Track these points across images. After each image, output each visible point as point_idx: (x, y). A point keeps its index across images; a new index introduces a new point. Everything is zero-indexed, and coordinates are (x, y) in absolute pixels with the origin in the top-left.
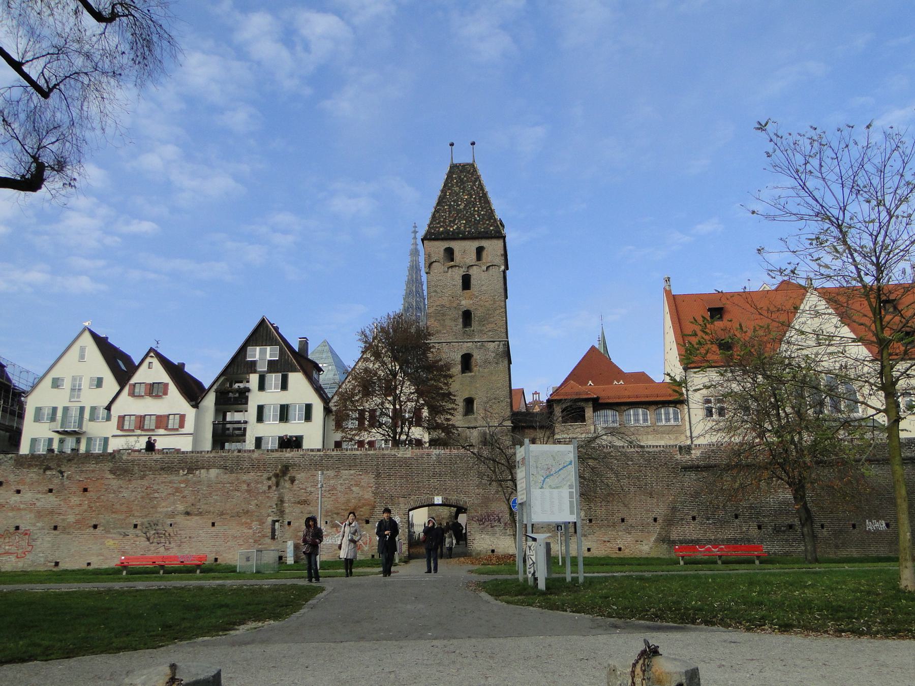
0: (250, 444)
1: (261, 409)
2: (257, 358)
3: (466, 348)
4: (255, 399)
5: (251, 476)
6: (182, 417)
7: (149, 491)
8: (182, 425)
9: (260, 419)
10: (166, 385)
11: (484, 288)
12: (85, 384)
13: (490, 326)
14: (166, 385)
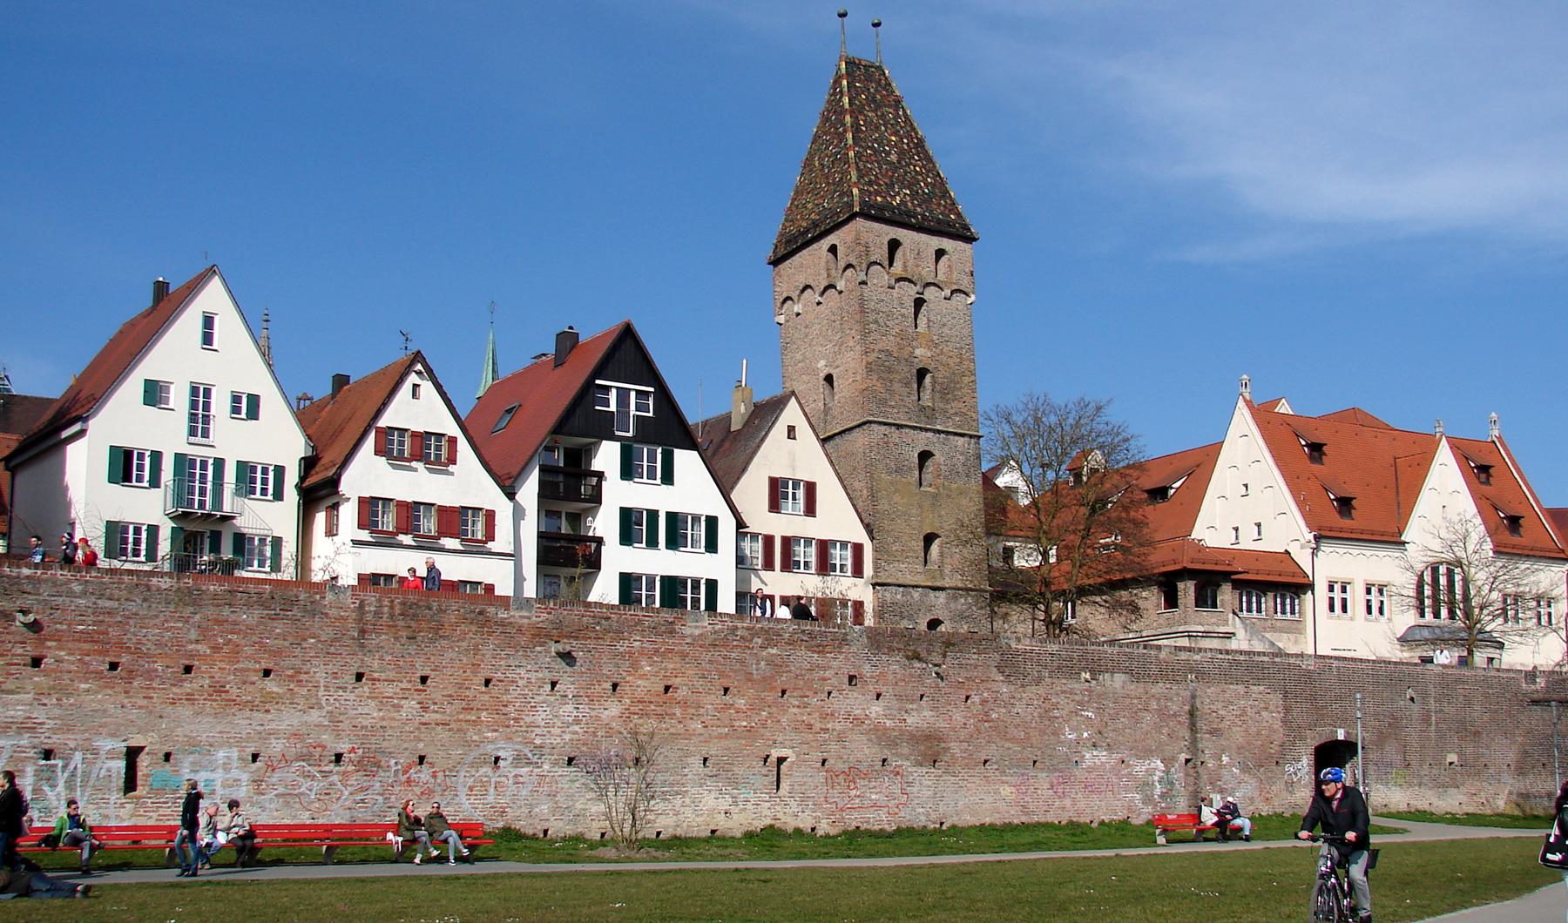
0: (605, 589)
2: (613, 407)
3: (923, 441)
4: (618, 494)
5: (1159, 689)
6: (490, 516)
7: (1047, 705)
8: (490, 536)
9: (627, 538)
10: (453, 441)
11: (946, 330)
12: (220, 405)
14: (453, 441)
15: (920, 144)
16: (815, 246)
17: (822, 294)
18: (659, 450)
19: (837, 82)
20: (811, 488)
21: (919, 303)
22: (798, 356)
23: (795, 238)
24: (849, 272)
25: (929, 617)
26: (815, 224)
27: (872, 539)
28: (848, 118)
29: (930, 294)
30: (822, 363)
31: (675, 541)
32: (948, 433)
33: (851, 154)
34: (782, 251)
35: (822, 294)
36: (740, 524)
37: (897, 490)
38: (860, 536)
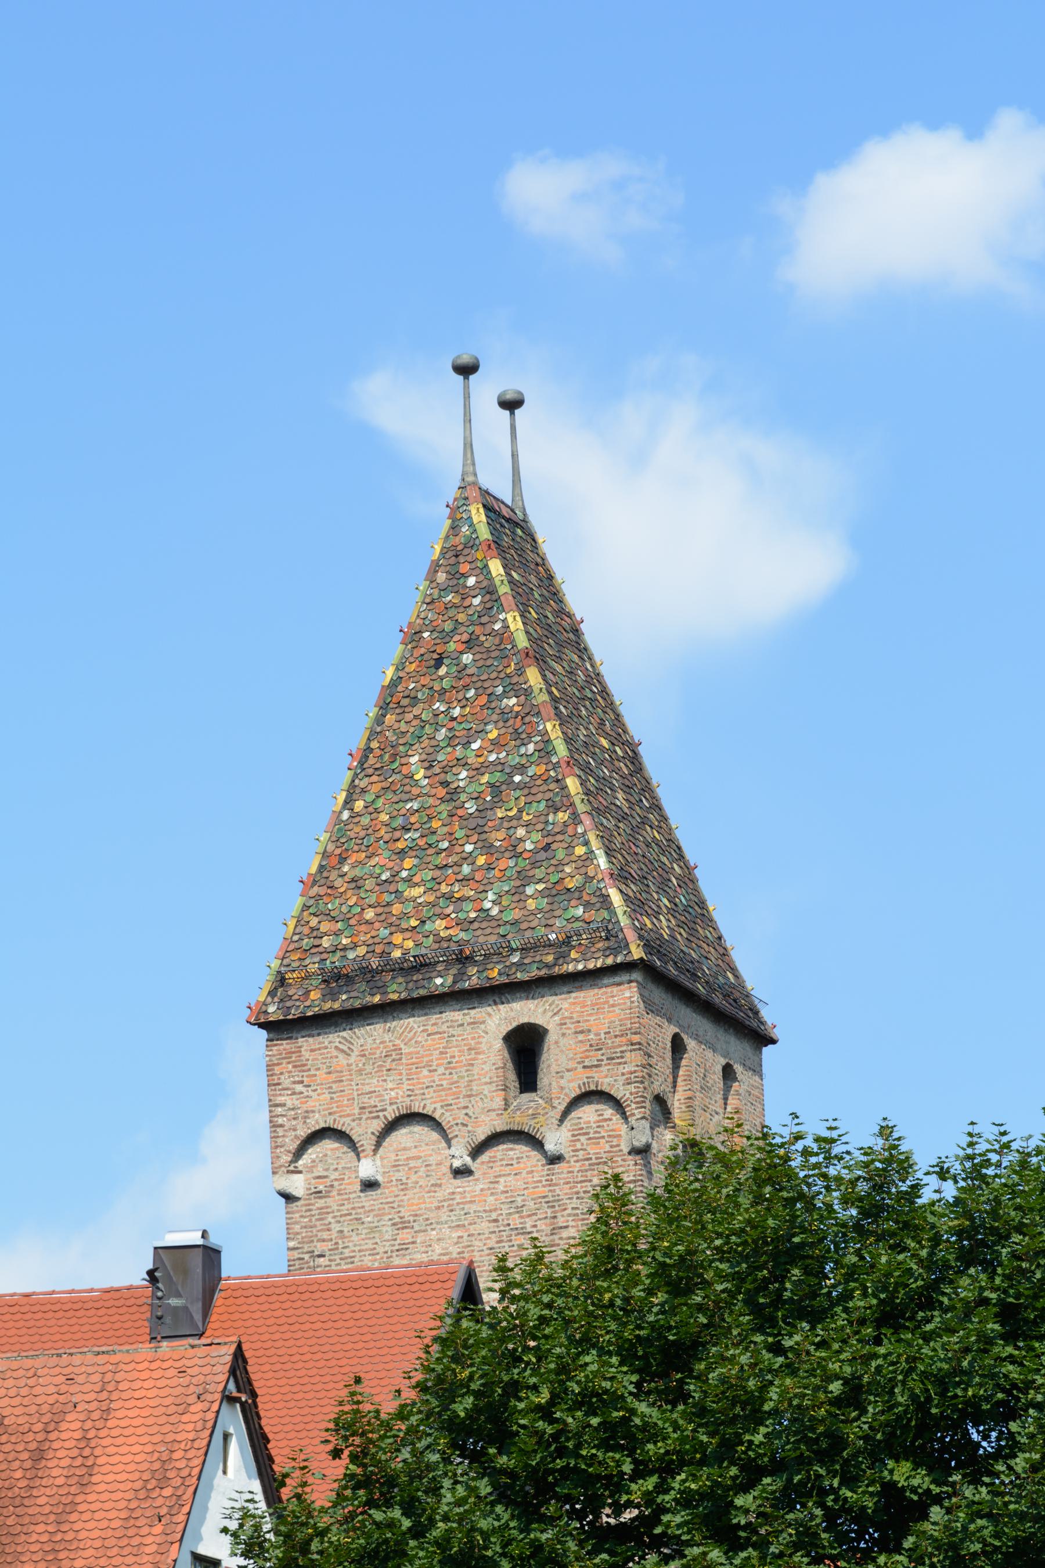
15: (634, 759)
17: (477, 1151)
19: (456, 554)
23: (368, 974)
24: (588, 1113)
26: (463, 960)
28: (533, 676)
33: (572, 784)
34: (316, 1002)
35: (477, 1151)
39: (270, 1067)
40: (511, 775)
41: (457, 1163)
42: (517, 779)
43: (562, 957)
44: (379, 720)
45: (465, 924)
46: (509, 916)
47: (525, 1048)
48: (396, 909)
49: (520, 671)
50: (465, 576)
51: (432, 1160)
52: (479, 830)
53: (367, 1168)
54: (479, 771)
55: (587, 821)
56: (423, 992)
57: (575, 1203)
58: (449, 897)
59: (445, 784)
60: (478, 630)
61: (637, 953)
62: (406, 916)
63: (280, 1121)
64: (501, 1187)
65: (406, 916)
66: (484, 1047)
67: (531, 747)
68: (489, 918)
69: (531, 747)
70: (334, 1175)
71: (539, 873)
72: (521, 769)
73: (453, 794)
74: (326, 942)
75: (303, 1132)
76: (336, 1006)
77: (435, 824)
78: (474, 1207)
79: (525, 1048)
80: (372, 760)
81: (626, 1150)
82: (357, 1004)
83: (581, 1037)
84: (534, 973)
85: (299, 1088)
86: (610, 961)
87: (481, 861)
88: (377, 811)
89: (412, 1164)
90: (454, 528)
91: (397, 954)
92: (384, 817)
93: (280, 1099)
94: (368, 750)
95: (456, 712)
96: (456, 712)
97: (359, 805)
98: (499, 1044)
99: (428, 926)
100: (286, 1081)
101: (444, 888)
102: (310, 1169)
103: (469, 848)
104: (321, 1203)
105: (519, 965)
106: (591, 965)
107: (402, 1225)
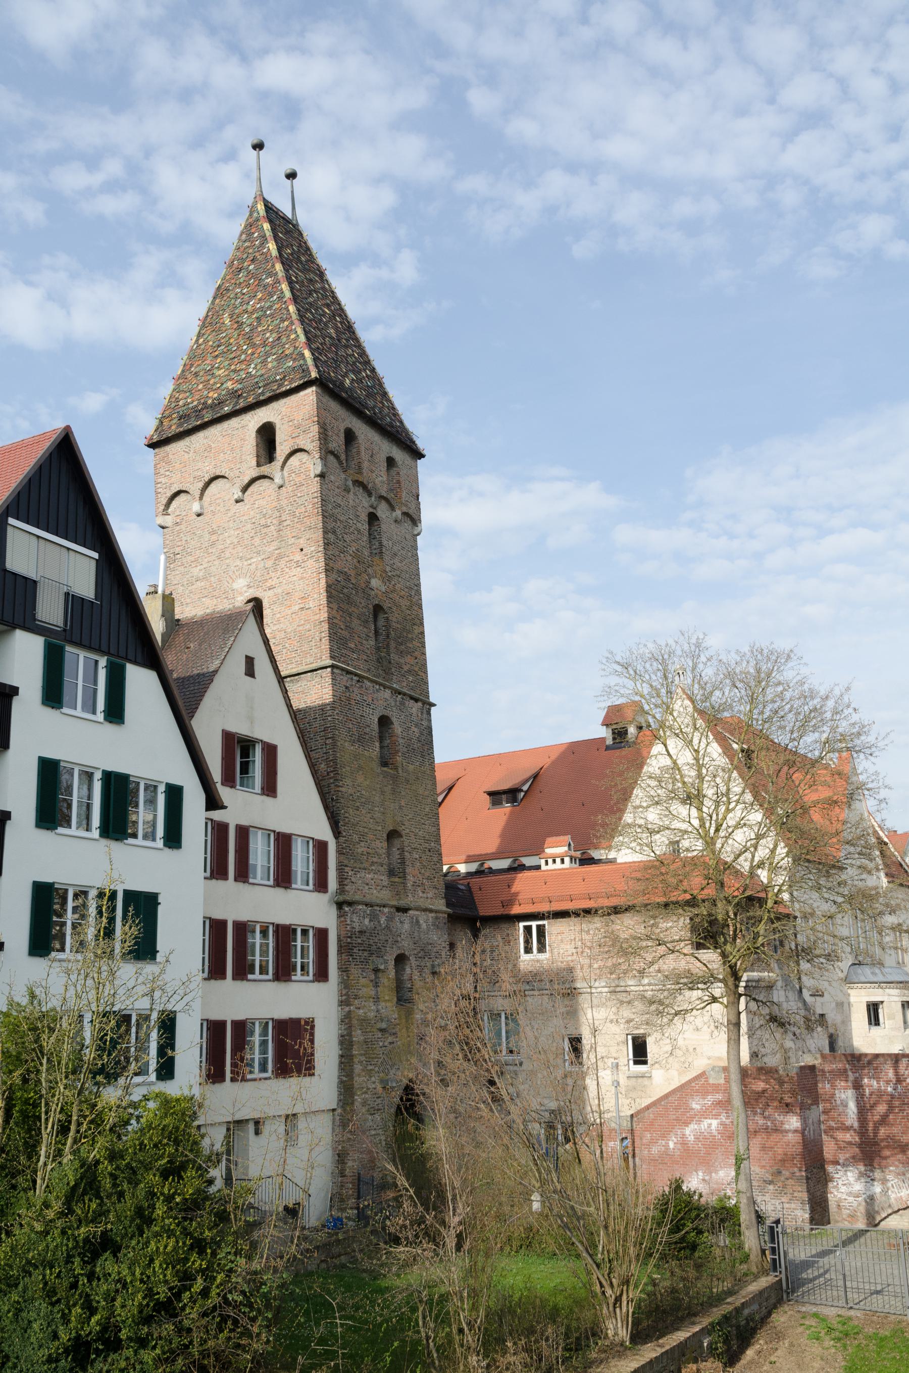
1: (50, 773)
9: (51, 814)
11: (396, 561)
13: (409, 659)
16: (234, 422)
17: (245, 489)
18: (103, 662)
19: (251, 225)
20: (271, 751)
21: (373, 518)
22: (196, 571)
23: (198, 412)
24: (294, 461)
25: (396, 952)
26: (235, 395)
27: (337, 834)
28: (278, 267)
29: (382, 511)
30: (240, 583)
31: (116, 826)
32: (405, 694)
34: (175, 429)
35: (245, 489)
36: (213, 802)
37: (360, 768)
38: (324, 832)
39: (155, 465)
40: (265, 312)
41: (236, 497)
42: (268, 312)
43: (280, 386)
44: (213, 303)
45: (240, 381)
46: (259, 373)
47: (267, 434)
48: (211, 382)
49: (273, 266)
50: (253, 233)
51: (226, 498)
52: (250, 338)
53: (196, 507)
54: (252, 313)
55: (297, 323)
56: (219, 415)
57: (290, 507)
58: (235, 371)
59: (238, 322)
60: (257, 254)
61: (314, 374)
62: (215, 383)
63: (159, 490)
64: (256, 506)
65: (215, 383)
66: (247, 437)
67: (275, 297)
68: (251, 376)
69: (275, 297)
70: (184, 513)
71: (274, 351)
72: (270, 308)
73: (240, 324)
74: (181, 403)
75: (169, 494)
76: (181, 429)
77: (231, 341)
78: (245, 518)
79: (267, 434)
80: (209, 320)
81: (312, 475)
82: (190, 427)
83: (291, 424)
84: (268, 394)
85: (168, 473)
86: (301, 382)
87: (250, 352)
88: (208, 341)
89: (218, 501)
90: (251, 215)
91: (210, 402)
92: (211, 343)
93: (159, 480)
94: (207, 316)
95: (244, 291)
96: (244, 291)
97: (201, 340)
98: (254, 435)
99: (224, 386)
100: (162, 471)
101: (233, 367)
102: (174, 512)
103: (245, 347)
104: (178, 528)
105: (263, 393)
106: (293, 386)
107: (213, 533)
